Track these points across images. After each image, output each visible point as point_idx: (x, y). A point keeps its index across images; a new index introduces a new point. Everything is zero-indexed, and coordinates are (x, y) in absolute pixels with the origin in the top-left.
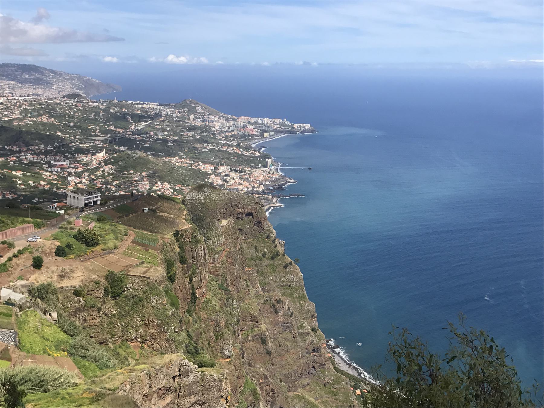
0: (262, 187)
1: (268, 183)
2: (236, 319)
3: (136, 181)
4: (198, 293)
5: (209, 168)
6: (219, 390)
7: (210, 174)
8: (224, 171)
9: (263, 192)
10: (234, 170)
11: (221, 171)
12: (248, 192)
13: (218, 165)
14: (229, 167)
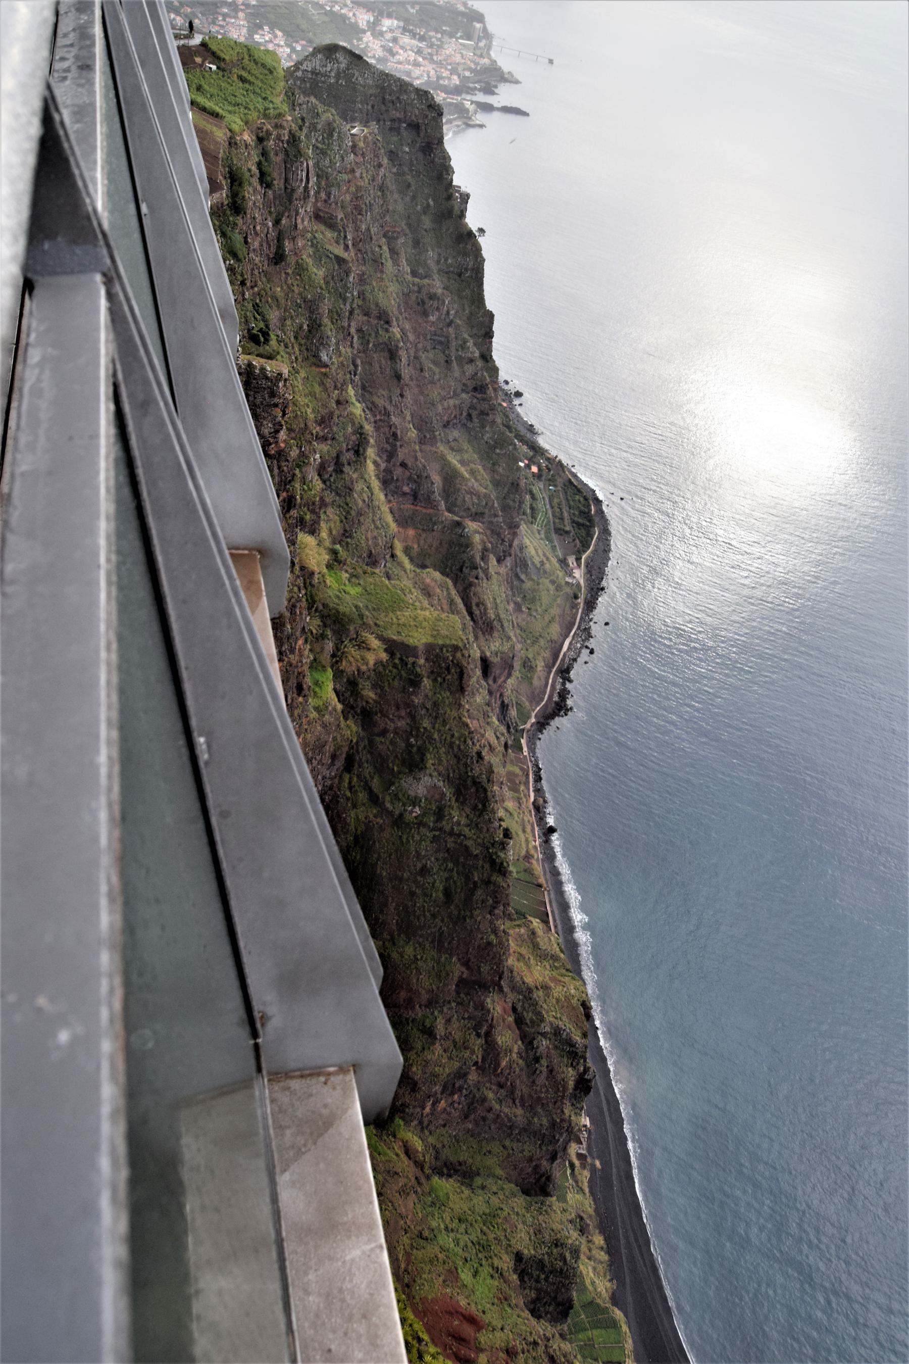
0: (456, 80)
1: (467, 74)
2: (348, 307)
3: (225, 16)
4: (288, 245)
5: (363, 18)
6: (273, 394)
7: (364, 32)
8: (391, 31)
9: (457, 91)
10: (410, 31)
11: (384, 29)
12: (428, 83)
13: (381, 14)
14: (401, 24)
